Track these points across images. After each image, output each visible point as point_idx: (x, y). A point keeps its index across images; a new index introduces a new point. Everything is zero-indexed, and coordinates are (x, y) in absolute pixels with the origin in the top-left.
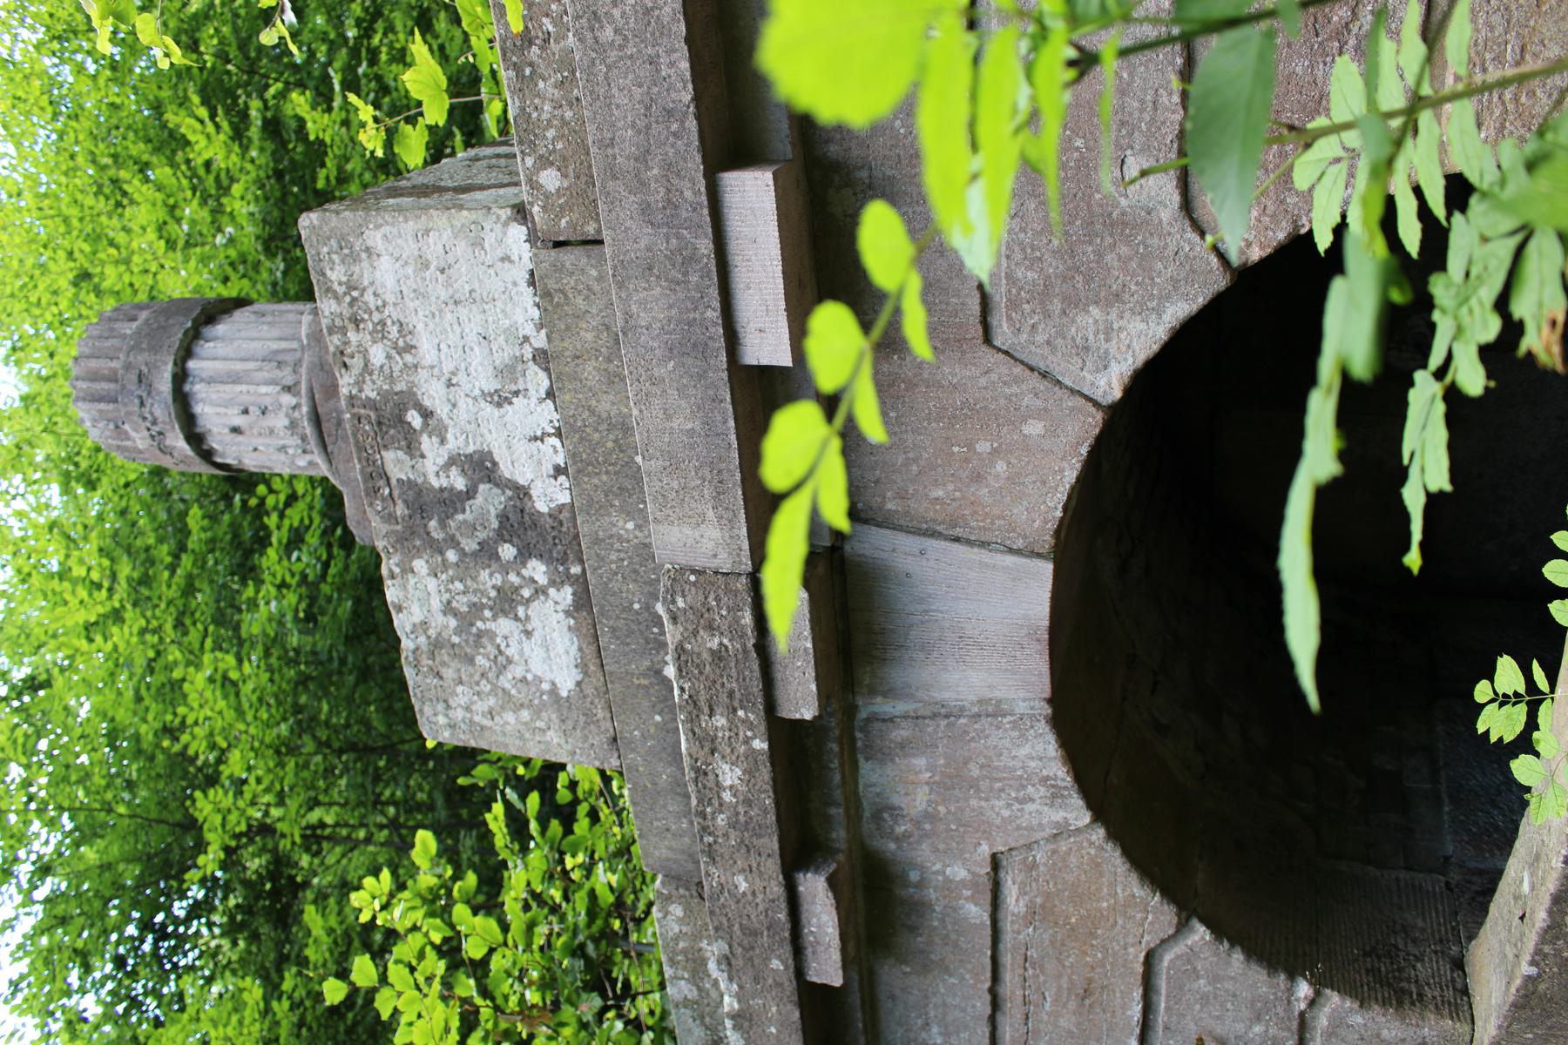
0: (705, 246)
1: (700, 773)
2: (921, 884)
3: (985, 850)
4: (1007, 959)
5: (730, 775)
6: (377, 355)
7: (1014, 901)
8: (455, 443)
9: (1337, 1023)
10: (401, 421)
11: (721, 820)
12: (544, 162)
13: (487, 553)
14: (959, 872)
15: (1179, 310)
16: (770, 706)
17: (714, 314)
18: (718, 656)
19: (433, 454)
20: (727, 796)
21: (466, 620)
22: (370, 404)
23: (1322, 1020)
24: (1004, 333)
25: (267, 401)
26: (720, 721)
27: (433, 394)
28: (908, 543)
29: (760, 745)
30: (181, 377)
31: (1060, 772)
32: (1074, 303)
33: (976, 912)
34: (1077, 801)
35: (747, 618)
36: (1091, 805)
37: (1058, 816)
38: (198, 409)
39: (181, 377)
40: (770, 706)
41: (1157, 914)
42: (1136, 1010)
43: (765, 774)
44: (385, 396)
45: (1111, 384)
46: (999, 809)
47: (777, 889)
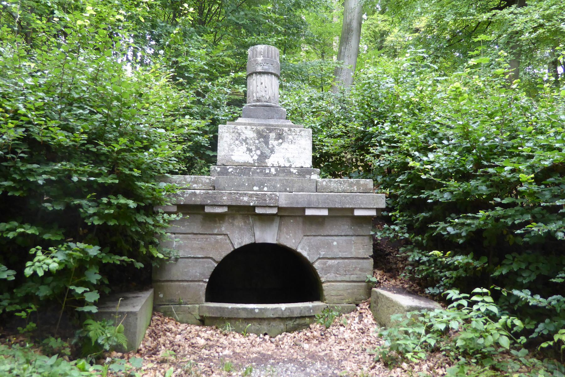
0: (320, 206)
1: (245, 194)
2: (220, 223)
3: (228, 233)
4: (206, 236)
5: (246, 199)
6: (290, 137)
7: (219, 237)
8: (277, 147)
9: (202, 286)
10: (280, 138)
11: (237, 196)
12: (327, 183)
13: (258, 148)
14: (223, 229)
15: (308, 258)
16: (258, 206)
17: (312, 206)
18: (265, 200)
19: (275, 143)
20: (241, 198)
21: (245, 140)
22: (283, 134)
23: (201, 283)
24: (305, 238)
25: (267, 92)
26: (255, 199)
27: (285, 145)
28: (278, 225)
29: (252, 204)
30: (272, 74)
31: (243, 244)
32: (309, 246)
33: (216, 231)
34: (239, 246)
35: (272, 205)
36: (238, 249)
37: (236, 244)
38: (266, 76)
39: (272, 74)
40: (258, 206)
41: (219, 258)
42: (200, 256)
43: (246, 204)
44: (284, 137)
45: (299, 250)
46: (237, 235)
47: (225, 204)
